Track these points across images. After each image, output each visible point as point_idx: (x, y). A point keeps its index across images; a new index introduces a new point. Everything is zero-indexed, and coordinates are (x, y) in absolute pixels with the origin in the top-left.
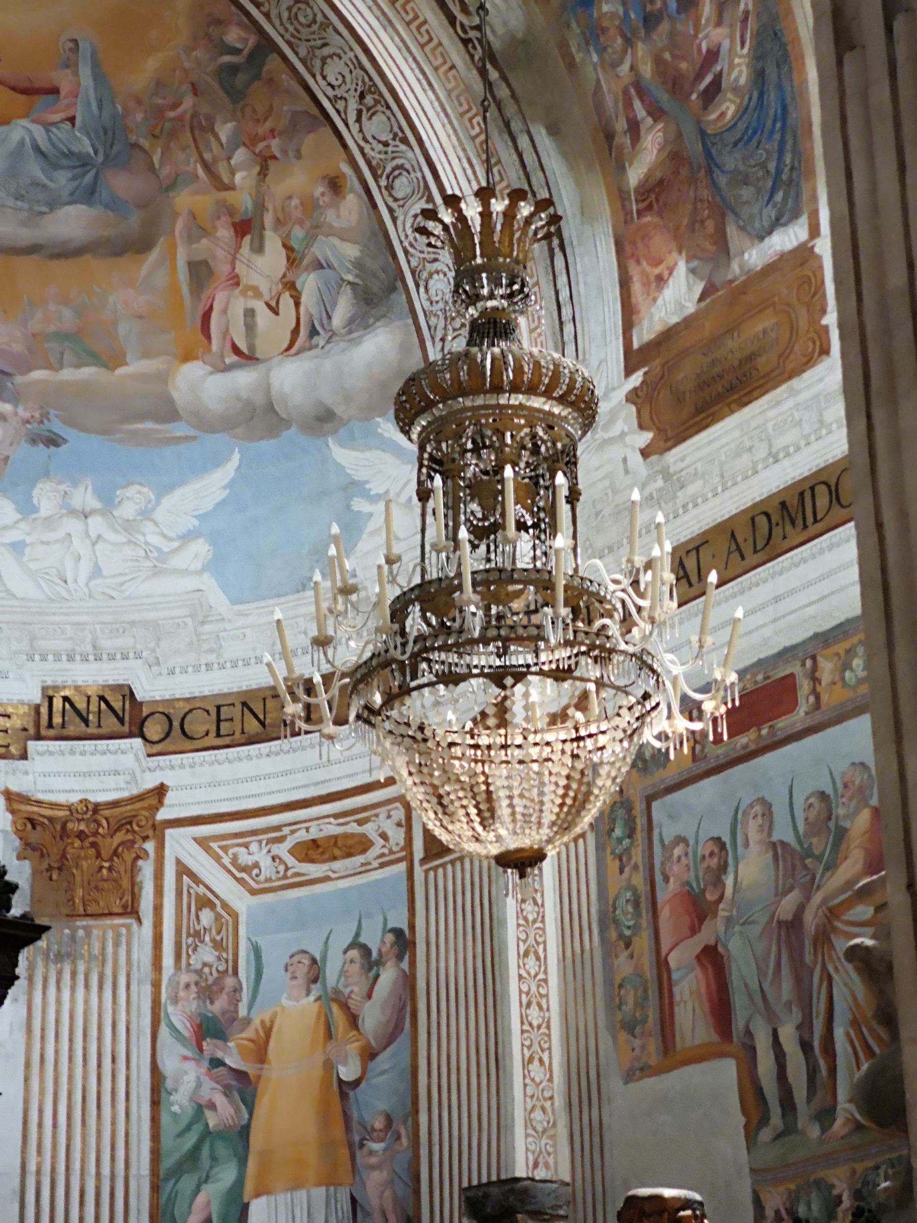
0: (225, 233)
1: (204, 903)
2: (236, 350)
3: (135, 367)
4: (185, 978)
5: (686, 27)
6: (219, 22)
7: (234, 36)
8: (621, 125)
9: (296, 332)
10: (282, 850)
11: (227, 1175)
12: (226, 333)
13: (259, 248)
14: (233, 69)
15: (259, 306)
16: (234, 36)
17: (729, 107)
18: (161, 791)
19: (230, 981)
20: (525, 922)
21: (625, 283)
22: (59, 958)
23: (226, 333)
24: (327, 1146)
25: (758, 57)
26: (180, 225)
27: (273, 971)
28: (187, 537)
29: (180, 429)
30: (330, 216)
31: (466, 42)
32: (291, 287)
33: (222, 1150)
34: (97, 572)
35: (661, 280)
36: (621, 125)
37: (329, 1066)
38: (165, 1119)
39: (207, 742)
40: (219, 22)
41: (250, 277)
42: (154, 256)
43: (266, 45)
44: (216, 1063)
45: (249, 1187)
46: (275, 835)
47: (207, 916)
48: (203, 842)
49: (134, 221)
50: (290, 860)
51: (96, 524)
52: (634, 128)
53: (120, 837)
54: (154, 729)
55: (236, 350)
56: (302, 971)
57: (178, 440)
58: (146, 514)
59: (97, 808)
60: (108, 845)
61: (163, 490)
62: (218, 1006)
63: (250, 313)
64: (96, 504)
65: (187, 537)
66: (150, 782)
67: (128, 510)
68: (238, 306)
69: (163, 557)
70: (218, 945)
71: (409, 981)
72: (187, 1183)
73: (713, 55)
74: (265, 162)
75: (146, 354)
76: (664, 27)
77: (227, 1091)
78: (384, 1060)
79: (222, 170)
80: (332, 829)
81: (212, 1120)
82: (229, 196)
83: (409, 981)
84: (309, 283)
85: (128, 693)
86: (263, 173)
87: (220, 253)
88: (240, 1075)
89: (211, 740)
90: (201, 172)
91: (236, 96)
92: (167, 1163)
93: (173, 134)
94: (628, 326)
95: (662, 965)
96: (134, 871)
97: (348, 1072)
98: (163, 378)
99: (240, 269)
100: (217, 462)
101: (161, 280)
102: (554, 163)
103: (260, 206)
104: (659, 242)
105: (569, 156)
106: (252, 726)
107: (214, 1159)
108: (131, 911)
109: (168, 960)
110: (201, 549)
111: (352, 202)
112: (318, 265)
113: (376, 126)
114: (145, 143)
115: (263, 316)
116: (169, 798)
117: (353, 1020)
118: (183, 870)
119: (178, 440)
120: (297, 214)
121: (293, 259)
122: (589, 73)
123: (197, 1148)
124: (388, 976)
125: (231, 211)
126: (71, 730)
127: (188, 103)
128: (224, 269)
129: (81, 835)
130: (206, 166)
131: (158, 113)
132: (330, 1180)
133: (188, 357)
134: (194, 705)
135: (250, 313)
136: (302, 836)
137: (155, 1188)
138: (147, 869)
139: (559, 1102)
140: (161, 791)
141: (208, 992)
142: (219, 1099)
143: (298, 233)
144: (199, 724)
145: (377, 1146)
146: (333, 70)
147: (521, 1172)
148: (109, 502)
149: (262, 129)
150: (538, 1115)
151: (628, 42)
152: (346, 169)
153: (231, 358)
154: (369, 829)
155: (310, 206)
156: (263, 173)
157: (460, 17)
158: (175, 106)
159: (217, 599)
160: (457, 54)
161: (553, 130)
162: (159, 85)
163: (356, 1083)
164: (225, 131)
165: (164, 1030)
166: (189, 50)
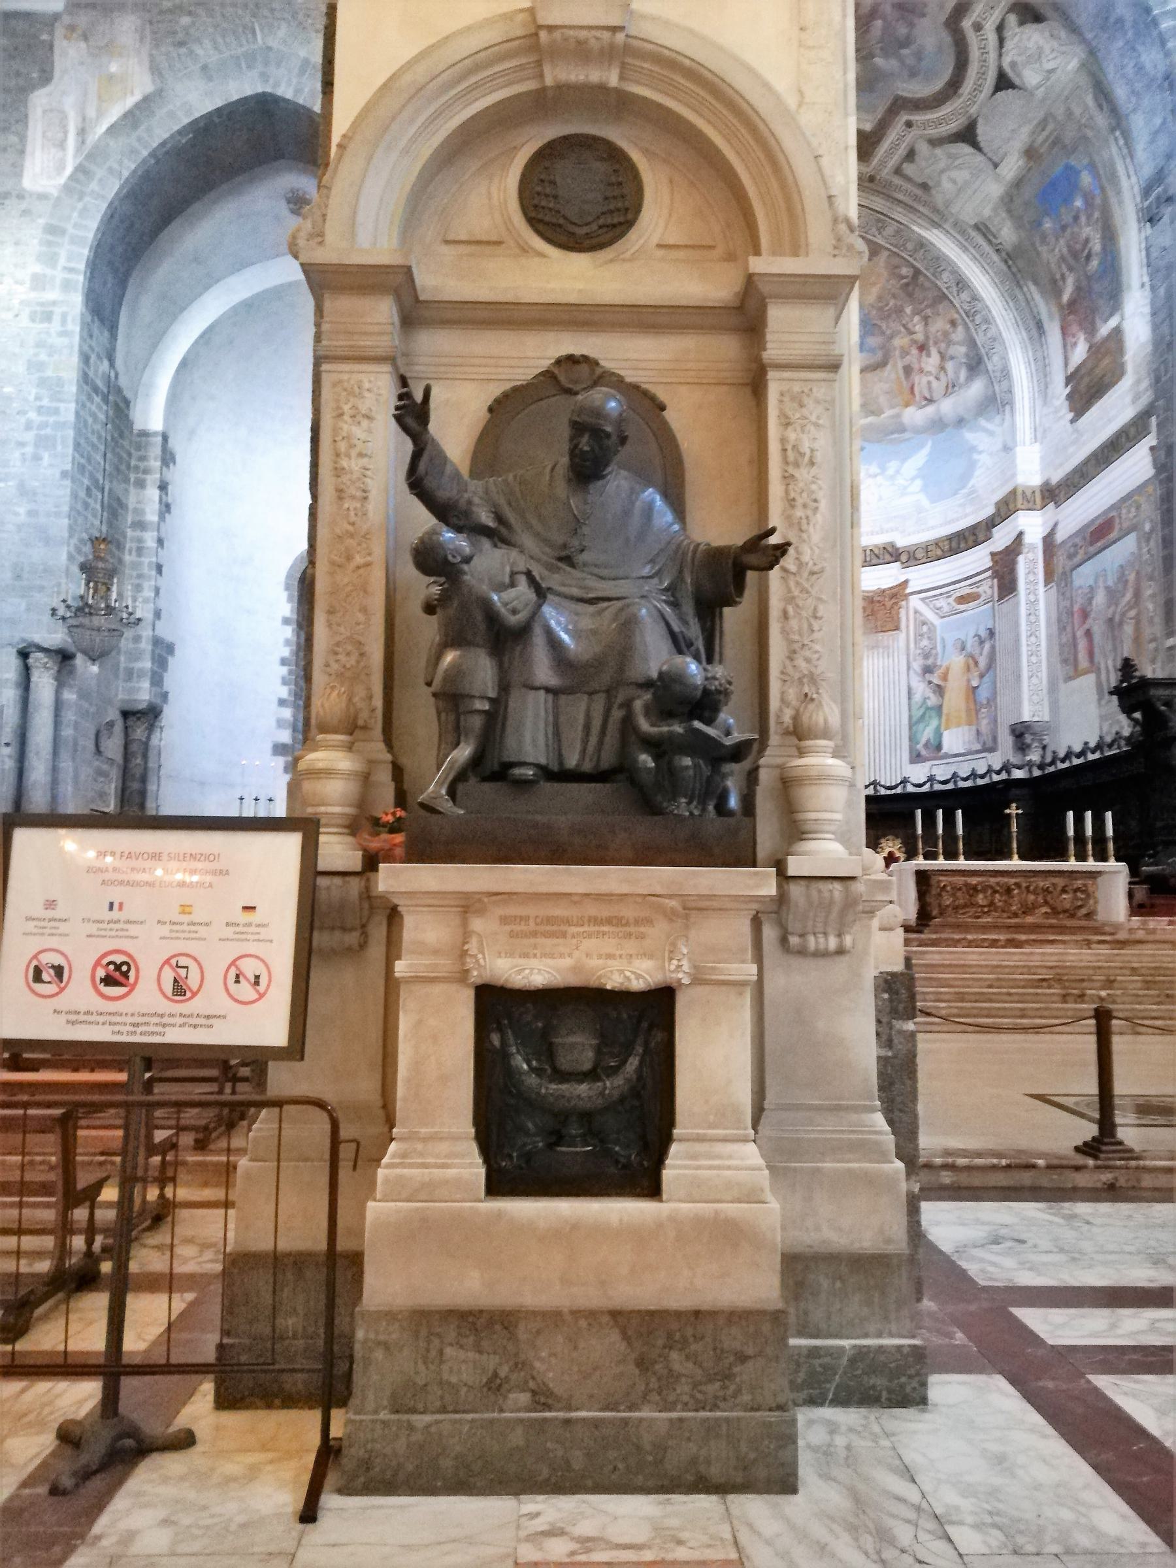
0: (914, 351)
1: (924, 623)
2: (926, 399)
3: (888, 413)
4: (919, 651)
5: (1076, 229)
6: (897, 267)
7: (905, 271)
8: (1058, 276)
9: (947, 387)
10: (951, 600)
11: (934, 723)
12: (921, 392)
13: (929, 355)
14: (907, 285)
15: (931, 378)
16: (905, 271)
17: (1095, 263)
18: (906, 582)
19: (934, 652)
20: (1030, 623)
21: (1065, 346)
22: (873, 648)
23: (921, 392)
24: (968, 710)
25: (1103, 238)
26: (897, 353)
27: (949, 647)
28: (913, 479)
29: (907, 435)
30: (954, 337)
31: (997, 251)
32: (942, 368)
33: (933, 713)
34: (880, 499)
35: (1075, 344)
36: (1058, 276)
37: (969, 681)
38: (913, 701)
39: (924, 560)
40: (897, 267)
41: (928, 368)
42: (889, 367)
43: (917, 272)
44: (930, 682)
45: (943, 728)
46: (947, 595)
47: (925, 628)
48: (923, 600)
49: (879, 355)
50: (954, 604)
51: (879, 479)
52: (1063, 278)
53: (893, 601)
54: (904, 558)
55: (926, 399)
56: (959, 646)
57: (908, 439)
58: (898, 472)
59: (884, 591)
60: (889, 604)
61: (904, 460)
62: (930, 662)
63: (929, 383)
64: (878, 471)
65: (913, 479)
66: (902, 579)
67: (890, 472)
68: (925, 380)
69: (905, 488)
70: (929, 638)
71: (993, 647)
72: (921, 726)
73: (1087, 241)
74: (926, 319)
75: (892, 407)
76: (1069, 231)
77: (934, 692)
78: (986, 679)
79: (910, 326)
80: (967, 591)
81: (929, 703)
82: (914, 336)
83: (993, 647)
84: (950, 366)
85: (892, 545)
86: (926, 324)
87: (915, 360)
88: (939, 686)
89: (924, 560)
90: (903, 329)
91: (910, 295)
92: (914, 719)
93: (889, 316)
94: (1066, 365)
95: (1074, 637)
96: (898, 613)
97: (975, 683)
98: (898, 416)
99: (923, 365)
100: (922, 446)
101: (893, 376)
102: (1037, 297)
103: (927, 337)
104: (1074, 328)
105: (1043, 293)
106: (939, 552)
107: (930, 717)
108: (897, 628)
109: (912, 645)
110: (918, 483)
111: (960, 329)
112: (952, 358)
113: (965, 296)
114: (878, 322)
115: (935, 384)
116: (910, 584)
117: (976, 663)
118: (916, 612)
119: (908, 439)
120: (941, 338)
121: (943, 357)
122: (1045, 255)
123: (924, 714)
124: (987, 646)
125: (914, 342)
126: (874, 562)
127: (892, 303)
128: (916, 366)
129: (879, 602)
130: (904, 326)
131: (881, 309)
132: (970, 724)
133: (907, 405)
134: (918, 547)
135: (929, 383)
136: (958, 594)
137: (910, 728)
138: (903, 612)
139: (1045, 691)
140: (906, 582)
141: (926, 656)
142: (931, 695)
143: (943, 345)
144: (919, 555)
145: (984, 710)
146: (945, 276)
147: (1026, 719)
148: (883, 469)
149: (923, 306)
150: (1035, 697)
151: (1057, 239)
152: (956, 316)
153: (924, 403)
154: (980, 590)
155: (946, 334)
156: (926, 324)
157: (994, 240)
158: (887, 305)
159: (925, 502)
160: (995, 258)
161: (1036, 283)
162: (880, 298)
163: (976, 688)
164: (908, 310)
165: (911, 672)
166: (888, 281)
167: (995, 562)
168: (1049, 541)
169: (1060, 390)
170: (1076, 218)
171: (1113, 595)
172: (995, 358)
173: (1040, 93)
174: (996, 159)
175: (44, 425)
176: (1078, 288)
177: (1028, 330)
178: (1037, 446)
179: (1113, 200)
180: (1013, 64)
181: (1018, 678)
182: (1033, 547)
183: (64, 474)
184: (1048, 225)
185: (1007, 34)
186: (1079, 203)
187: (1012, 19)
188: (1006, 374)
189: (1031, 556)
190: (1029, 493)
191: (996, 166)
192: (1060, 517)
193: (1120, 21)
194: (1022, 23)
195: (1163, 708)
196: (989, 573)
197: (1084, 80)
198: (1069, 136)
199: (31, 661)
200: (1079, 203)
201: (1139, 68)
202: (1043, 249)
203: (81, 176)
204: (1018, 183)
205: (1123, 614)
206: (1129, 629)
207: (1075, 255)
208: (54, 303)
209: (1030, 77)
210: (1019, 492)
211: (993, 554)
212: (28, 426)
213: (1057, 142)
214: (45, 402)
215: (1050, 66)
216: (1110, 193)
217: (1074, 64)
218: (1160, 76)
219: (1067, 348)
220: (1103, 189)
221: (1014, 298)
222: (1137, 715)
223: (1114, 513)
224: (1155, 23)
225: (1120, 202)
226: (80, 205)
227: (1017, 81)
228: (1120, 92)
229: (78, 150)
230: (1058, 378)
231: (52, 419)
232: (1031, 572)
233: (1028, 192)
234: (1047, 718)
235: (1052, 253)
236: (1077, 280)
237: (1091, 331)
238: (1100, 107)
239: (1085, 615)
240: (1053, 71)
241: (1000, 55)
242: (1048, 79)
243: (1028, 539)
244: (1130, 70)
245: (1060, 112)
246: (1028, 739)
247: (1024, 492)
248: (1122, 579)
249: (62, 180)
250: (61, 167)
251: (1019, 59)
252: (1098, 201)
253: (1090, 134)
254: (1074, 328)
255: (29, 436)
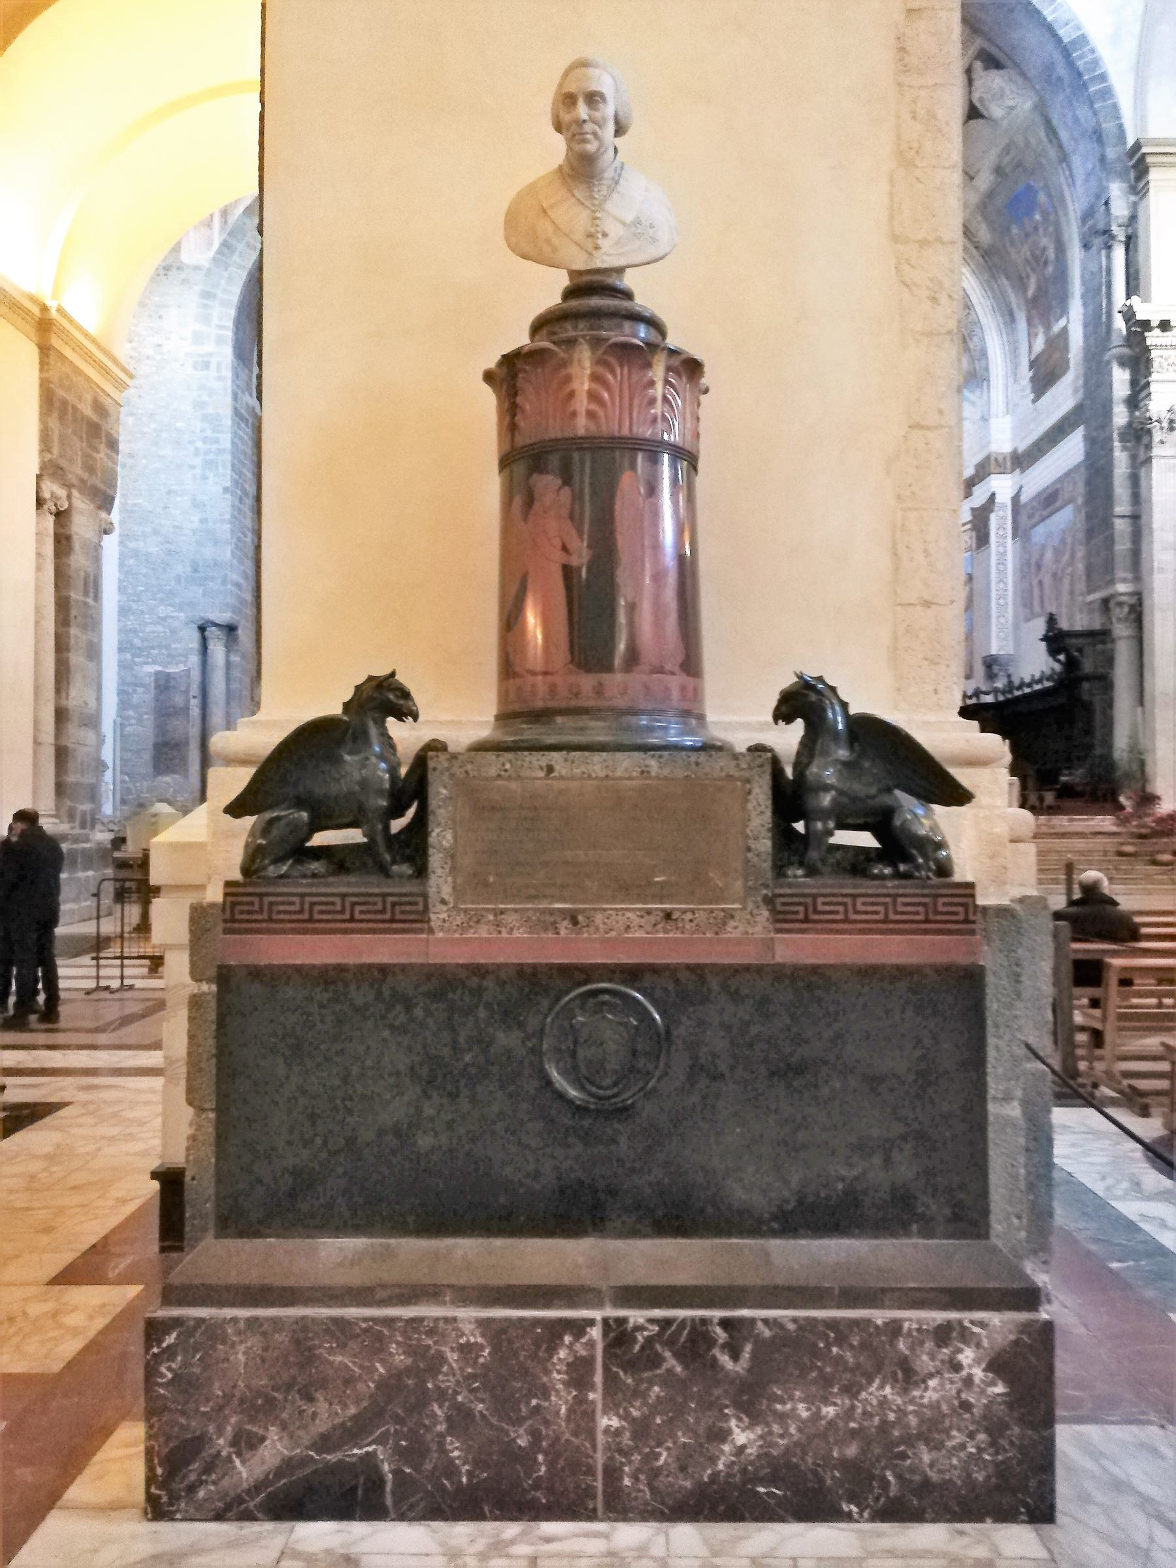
8: (1024, 275)
20: (999, 571)
21: (1029, 335)
35: (1036, 335)
52: (1028, 276)
94: (1030, 352)
95: (1031, 585)
102: (1009, 290)
104: (1036, 321)
105: (1013, 287)
139: (1010, 629)
147: (994, 652)
161: (1007, 278)
167: (974, 516)
168: (1016, 499)
169: (1026, 374)
170: (1036, 229)
171: (1058, 553)
172: (975, 339)
173: (1005, 123)
174: (972, 173)
175: (207, 453)
176: (1039, 288)
177: (1003, 315)
178: (1008, 418)
179: (1063, 219)
180: (981, 100)
181: (989, 617)
182: (1004, 506)
183: (226, 490)
184: (1015, 230)
185: (975, 76)
186: (1038, 217)
187: (978, 65)
188: (984, 353)
189: (1001, 513)
190: (1000, 459)
191: (972, 178)
192: (1023, 482)
193: (1060, 79)
194: (986, 68)
195: (1076, 654)
196: (968, 526)
197: (1038, 120)
198: (1029, 160)
199: (207, 633)
200: (1038, 217)
201: (1076, 120)
202: (1012, 251)
203: (226, 251)
204: (991, 195)
205: (1063, 570)
206: (1066, 582)
207: (1036, 258)
208: (211, 355)
209: (996, 111)
210: (992, 458)
211: (973, 509)
212: (197, 453)
213: (1019, 165)
214: (208, 433)
215: (1010, 103)
216: (1061, 213)
217: (1028, 105)
218: (1090, 130)
219: (1031, 336)
220: (1054, 207)
221: (992, 289)
222: (1062, 657)
223: (1059, 486)
224: (1085, 86)
225: (1068, 222)
226: (226, 274)
227: (985, 113)
228: (1064, 135)
229: (222, 229)
230: (1025, 363)
231: (214, 447)
232: (1001, 527)
233: (1000, 201)
234: (1011, 652)
235: (1020, 254)
236: (1038, 281)
237: (1048, 328)
238: (1051, 141)
239: (1039, 567)
240: (1012, 108)
241: (970, 92)
242: (1009, 114)
243: (998, 499)
244: (1070, 122)
245: (1020, 140)
246: (996, 669)
247: (996, 460)
248: (1063, 541)
249: (211, 254)
250: (210, 243)
251: (985, 96)
252: (1052, 218)
253: (1044, 161)
254: (1036, 321)
255: (198, 461)
